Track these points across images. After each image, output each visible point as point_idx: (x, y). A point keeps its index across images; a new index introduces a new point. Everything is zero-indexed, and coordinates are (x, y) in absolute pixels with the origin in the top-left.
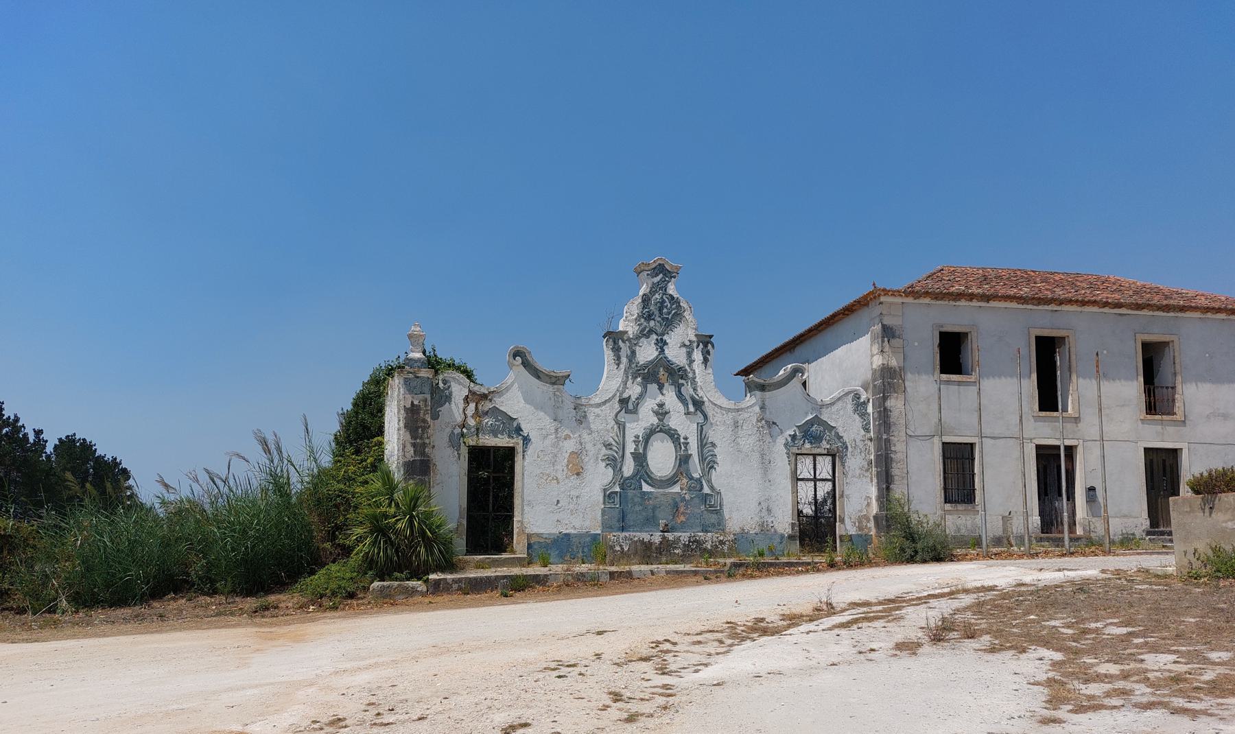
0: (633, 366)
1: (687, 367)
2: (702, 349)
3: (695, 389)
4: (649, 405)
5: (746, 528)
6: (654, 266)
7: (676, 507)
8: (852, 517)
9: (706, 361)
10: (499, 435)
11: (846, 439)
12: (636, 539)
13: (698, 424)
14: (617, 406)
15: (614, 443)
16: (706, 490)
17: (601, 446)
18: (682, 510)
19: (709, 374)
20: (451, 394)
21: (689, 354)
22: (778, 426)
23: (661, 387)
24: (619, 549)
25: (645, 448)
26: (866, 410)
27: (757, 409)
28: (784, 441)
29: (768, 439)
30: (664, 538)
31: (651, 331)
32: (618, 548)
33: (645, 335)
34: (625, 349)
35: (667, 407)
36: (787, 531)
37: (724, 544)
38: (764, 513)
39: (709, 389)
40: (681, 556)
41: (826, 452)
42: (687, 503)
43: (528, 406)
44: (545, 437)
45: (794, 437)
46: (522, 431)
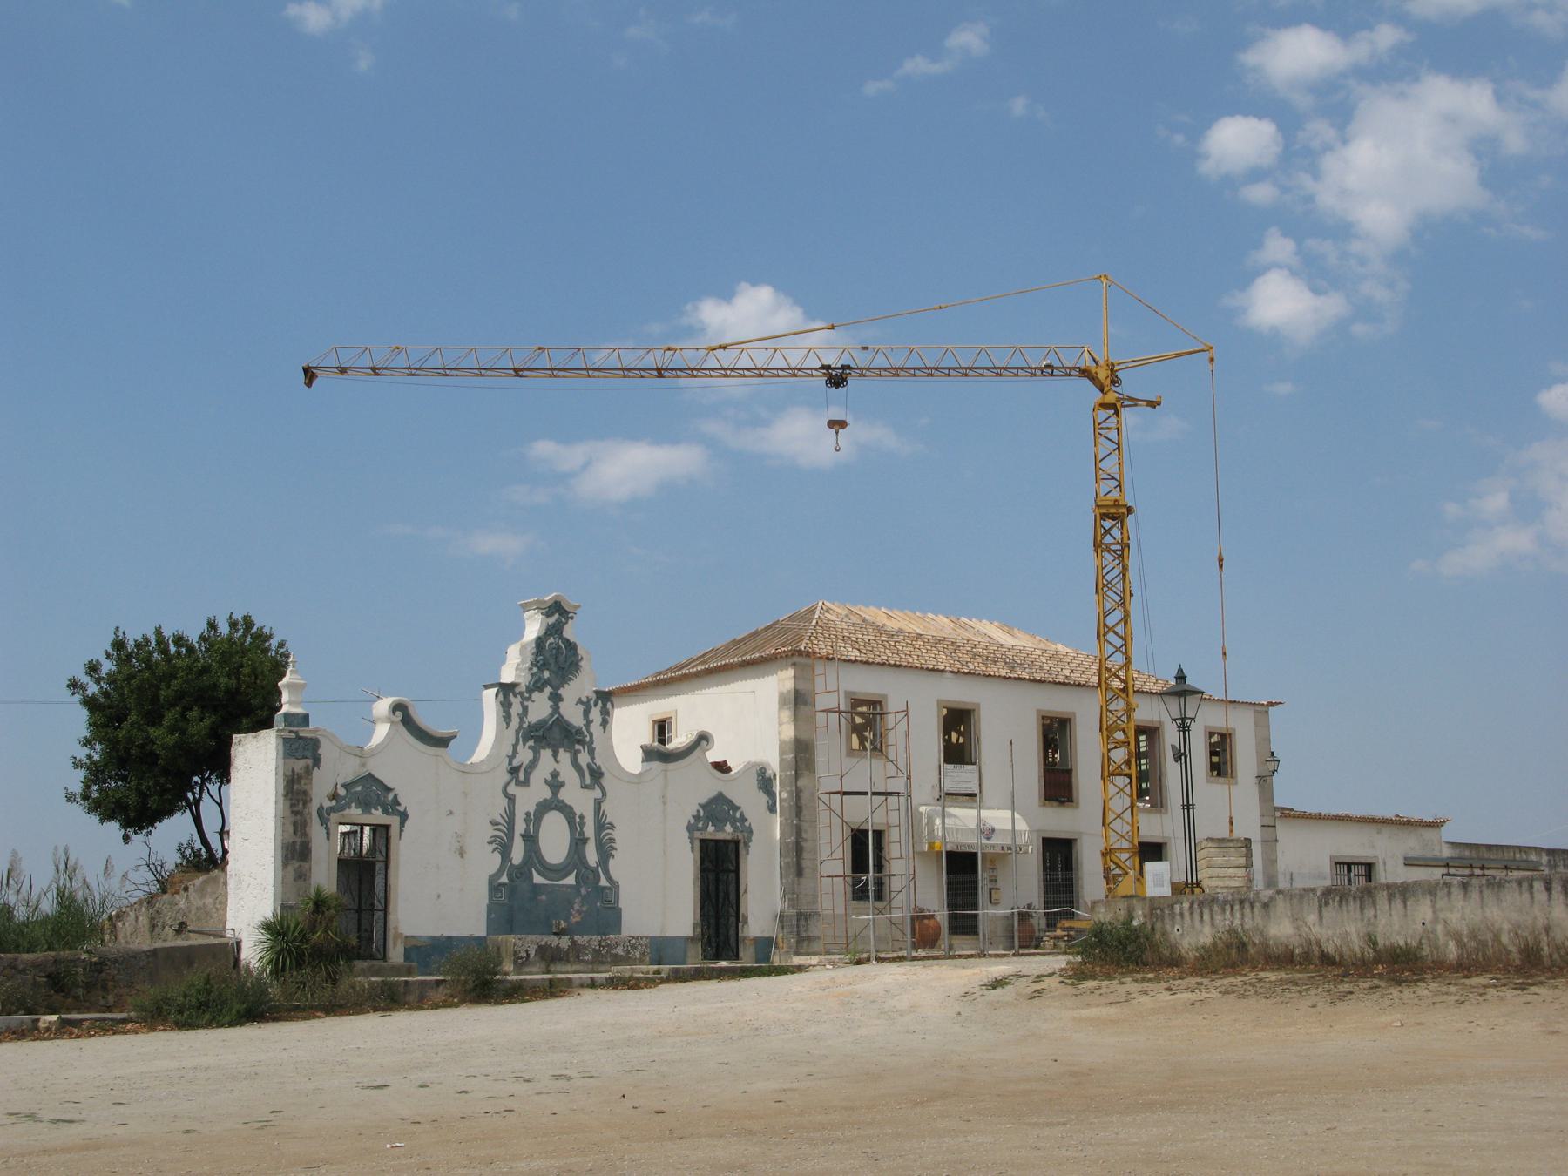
1: (584, 729)
3: (593, 758)
10: (373, 811)
12: (543, 943)
14: (507, 777)
16: (603, 882)
23: (555, 755)
30: (574, 942)
31: (547, 682)
34: (516, 703)
35: (560, 779)
37: (636, 948)
46: (399, 804)
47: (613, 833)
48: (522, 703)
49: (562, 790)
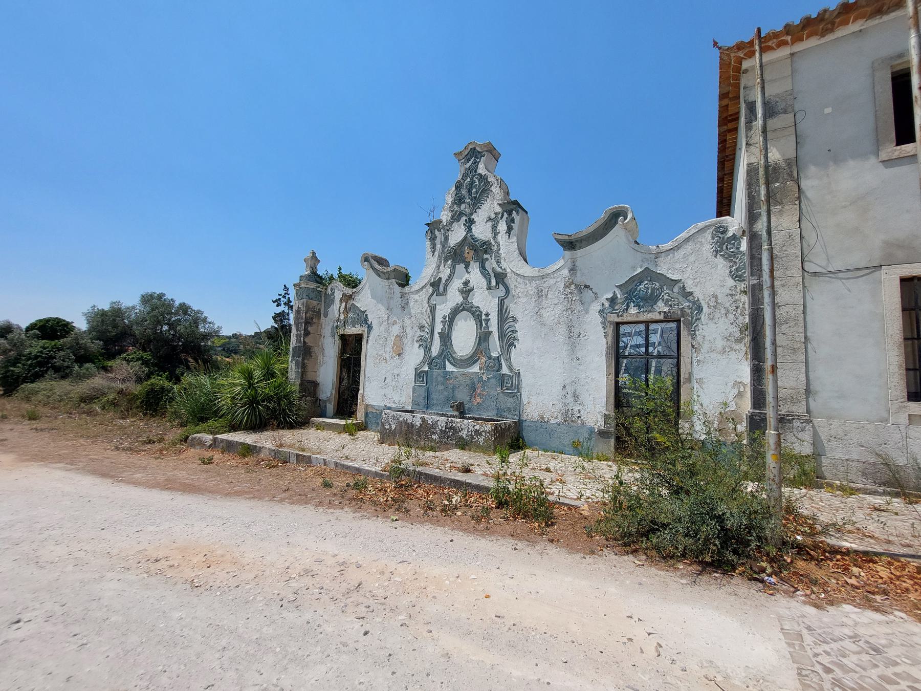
0: (446, 250)
1: (492, 241)
2: (507, 218)
3: (498, 262)
4: (457, 284)
5: (547, 416)
7: (473, 388)
9: (510, 229)
10: (356, 326)
11: (698, 294)
12: (401, 419)
13: (499, 298)
14: (431, 290)
15: (426, 325)
16: (505, 370)
17: (416, 328)
18: (479, 391)
19: (513, 243)
20: (334, 298)
21: (494, 227)
23: (467, 267)
24: (388, 427)
25: (450, 327)
26: (738, 248)
27: (565, 272)
28: (599, 307)
29: (579, 307)
30: (424, 420)
31: (461, 214)
33: (455, 219)
35: (471, 285)
36: (599, 424)
37: (480, 434)
38: (570, 399)
39: (512, 259)
40: (438, 443)
41: (662, 317)
42: (484, 383)
43: (372, 300)
44: (381, 325)
45: (613, 300)
47: (516, 325)
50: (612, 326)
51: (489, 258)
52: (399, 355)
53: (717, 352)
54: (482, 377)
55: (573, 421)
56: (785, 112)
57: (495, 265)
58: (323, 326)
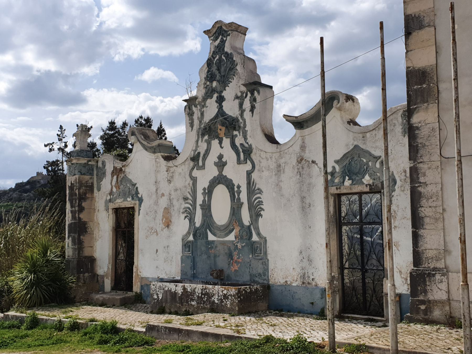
1: (240, 118)
2: (250, 97)
4: (212, 158)
5: (289, 280)
6: (214, 31)
7: (230, 256)
8: (403, 271)
9: (253, 109)
12: (166, 289)
14: (192, 164)
18: (235, 257)
21: (241, 105)
22: (317, 164)
23: (220, 143)
30: (184, 289)
32: (155, 297)
33: (208, 96)
35: (224, 160)
37: (228, 298)
47: (261, 197)
48: (200, 110)
49: (226, 168)
50: (333, 198)
51: (238, 134)
52: (168, 226)
53: (408, 219)
54: (237, 246)
55: (309, 283)
56: (429, 26)
57: (242, 141)
58: (97, 200)
